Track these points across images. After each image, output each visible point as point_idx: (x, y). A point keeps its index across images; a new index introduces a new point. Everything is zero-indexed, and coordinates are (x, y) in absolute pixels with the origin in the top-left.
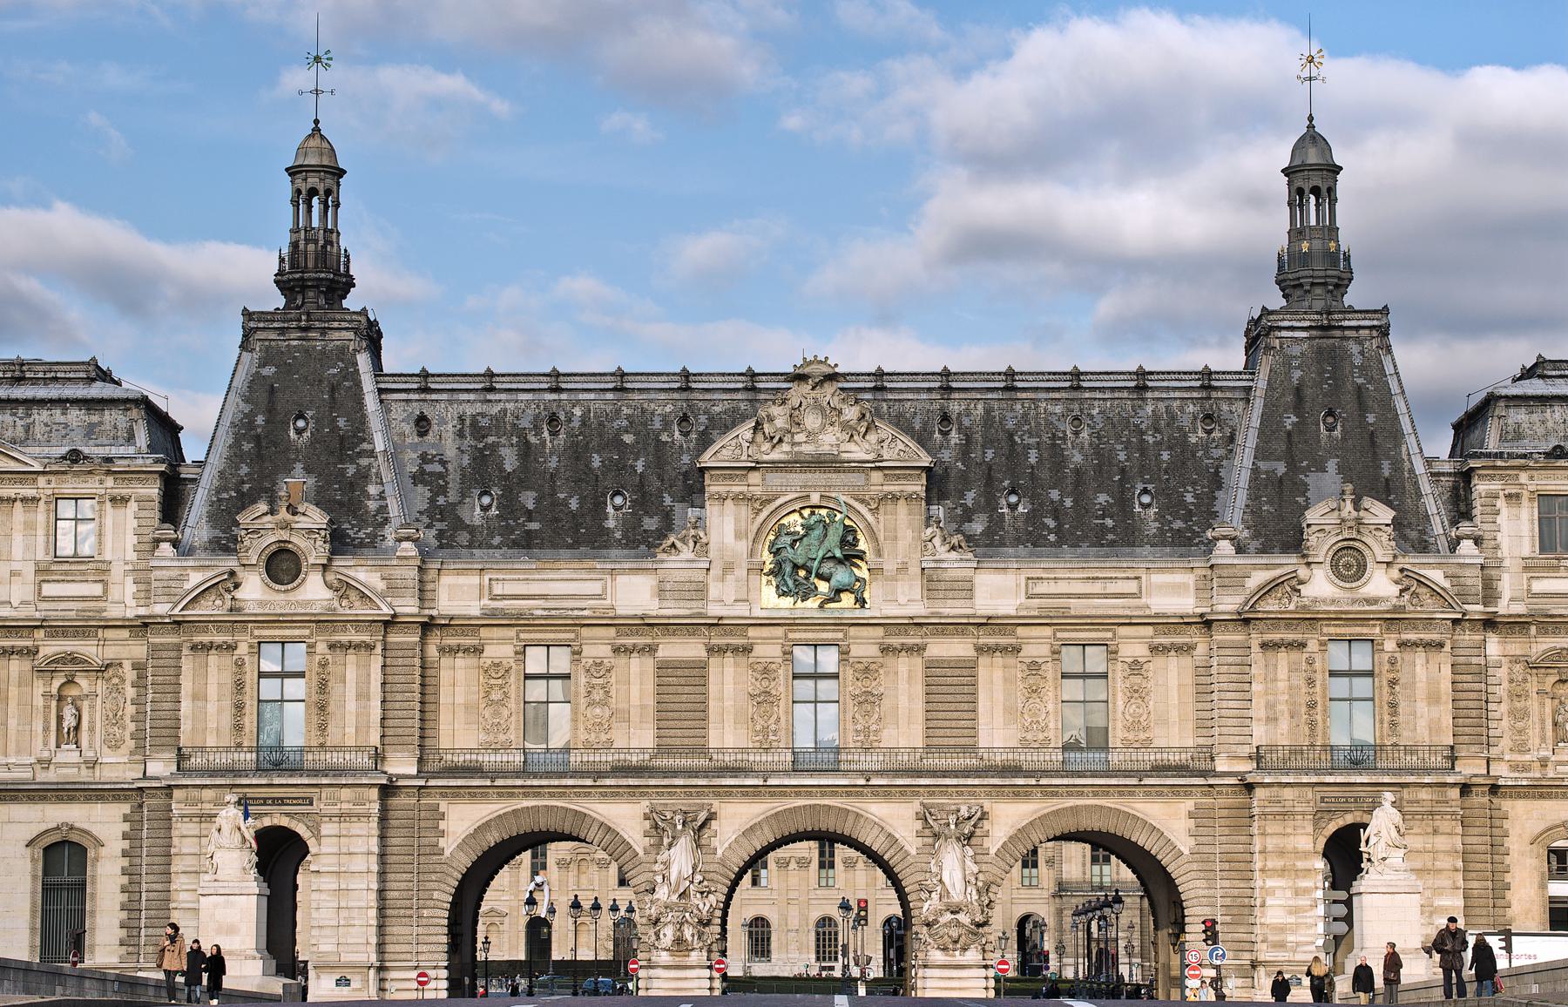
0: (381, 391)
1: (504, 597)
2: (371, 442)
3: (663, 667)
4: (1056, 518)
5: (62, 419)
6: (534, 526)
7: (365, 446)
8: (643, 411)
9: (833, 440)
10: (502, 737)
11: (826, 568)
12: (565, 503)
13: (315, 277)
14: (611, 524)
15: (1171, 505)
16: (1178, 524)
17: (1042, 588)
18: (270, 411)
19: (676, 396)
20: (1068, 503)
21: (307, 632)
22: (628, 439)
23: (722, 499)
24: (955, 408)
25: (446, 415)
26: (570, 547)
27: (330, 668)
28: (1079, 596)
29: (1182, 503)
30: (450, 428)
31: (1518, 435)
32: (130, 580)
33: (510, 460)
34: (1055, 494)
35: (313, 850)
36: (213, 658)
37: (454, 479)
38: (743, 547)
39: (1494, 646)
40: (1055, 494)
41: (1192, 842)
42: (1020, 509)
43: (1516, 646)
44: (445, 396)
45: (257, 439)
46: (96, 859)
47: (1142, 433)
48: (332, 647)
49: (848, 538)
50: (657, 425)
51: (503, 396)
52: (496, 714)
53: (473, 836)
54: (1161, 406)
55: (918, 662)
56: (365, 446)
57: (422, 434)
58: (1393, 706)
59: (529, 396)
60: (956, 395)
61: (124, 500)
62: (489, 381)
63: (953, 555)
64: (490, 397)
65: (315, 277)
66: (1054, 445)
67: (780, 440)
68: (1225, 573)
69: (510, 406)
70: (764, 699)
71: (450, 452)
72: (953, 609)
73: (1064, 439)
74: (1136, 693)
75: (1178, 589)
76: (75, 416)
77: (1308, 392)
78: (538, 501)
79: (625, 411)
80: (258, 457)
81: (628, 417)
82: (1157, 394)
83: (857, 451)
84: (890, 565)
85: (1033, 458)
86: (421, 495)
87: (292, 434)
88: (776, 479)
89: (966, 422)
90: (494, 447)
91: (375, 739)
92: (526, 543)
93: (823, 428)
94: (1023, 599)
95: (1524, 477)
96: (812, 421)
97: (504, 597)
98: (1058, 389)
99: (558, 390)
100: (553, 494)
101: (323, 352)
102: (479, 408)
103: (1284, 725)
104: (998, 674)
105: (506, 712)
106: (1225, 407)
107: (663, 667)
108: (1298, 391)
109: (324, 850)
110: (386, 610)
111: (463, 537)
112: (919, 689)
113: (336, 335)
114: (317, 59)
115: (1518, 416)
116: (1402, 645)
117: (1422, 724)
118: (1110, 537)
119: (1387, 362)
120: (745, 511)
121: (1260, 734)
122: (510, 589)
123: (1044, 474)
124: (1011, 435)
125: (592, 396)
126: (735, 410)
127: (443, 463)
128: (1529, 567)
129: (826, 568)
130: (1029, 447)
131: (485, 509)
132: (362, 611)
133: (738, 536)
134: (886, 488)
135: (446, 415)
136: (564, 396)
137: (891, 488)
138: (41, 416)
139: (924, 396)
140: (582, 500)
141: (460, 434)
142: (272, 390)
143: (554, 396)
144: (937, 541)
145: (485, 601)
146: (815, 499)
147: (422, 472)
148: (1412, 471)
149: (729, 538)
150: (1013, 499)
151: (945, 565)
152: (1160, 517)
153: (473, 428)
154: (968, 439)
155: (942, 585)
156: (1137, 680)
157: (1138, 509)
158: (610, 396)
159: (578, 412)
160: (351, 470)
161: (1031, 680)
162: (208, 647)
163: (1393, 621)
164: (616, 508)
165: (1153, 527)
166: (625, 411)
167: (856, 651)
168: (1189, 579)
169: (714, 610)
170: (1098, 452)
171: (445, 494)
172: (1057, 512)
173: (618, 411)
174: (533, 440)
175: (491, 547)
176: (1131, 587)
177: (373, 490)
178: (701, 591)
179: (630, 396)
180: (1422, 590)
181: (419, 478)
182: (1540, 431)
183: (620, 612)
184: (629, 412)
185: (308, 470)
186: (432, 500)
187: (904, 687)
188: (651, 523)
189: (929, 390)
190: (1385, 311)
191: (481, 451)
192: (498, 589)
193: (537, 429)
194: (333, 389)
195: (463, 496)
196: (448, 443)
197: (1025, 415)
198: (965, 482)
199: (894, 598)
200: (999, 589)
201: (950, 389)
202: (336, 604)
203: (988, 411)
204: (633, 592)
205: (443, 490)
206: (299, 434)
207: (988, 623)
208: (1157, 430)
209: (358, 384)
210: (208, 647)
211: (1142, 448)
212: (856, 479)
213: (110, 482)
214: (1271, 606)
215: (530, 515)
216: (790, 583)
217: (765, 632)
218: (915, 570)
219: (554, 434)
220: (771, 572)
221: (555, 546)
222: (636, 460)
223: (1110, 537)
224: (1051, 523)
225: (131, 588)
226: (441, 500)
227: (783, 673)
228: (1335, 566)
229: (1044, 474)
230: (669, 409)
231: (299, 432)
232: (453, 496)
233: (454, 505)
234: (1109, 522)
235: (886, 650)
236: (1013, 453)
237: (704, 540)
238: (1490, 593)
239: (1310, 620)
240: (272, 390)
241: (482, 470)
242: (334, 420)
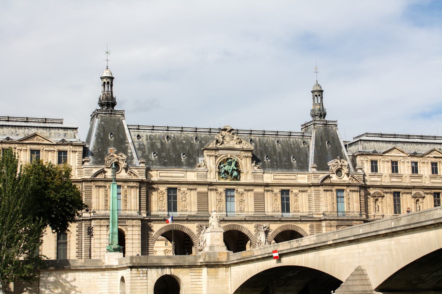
0: (129, 129)
1: (162, 176)
2: (128, 140)
3: (199, 193)
5: (58, 132)
6: (166, 161)
7: (127, 141)
10: (163, 209)
12: (172, 156)
13: (108, 103)
14: (183, 161)
15: (299, 161)
16: (300, 164)
17: (277, 177)
18: (104, 132)
19: (193, 133)
20: (278, 159)
21: (122, 183)
22: (184, 142)
24: (253, 138)
25: (144, 134)
26: (174, 166)
27: (127, 192)
28: (284, 179)
29: (301, 160)
30: (144, 138)
31: (366, 148)
32: (76, 170)
33: (159, 145)
34: (275, 157)
35: (126, 233)
36: (101, 189)
37: (146, 149)
40: (275, 157)
41: (310, 232)
44: (142, 131)
45: (102, 139)
46: (70, 236)
47: (291, 145)
48: (128, 187)
49: (237, 164)
50: (190, 139)
51: (156, 131)
52: (162, 203)
53: (159, 231)
54: (294, 139)
56: (127, 141)
57: (138, 139)
58: (349, 203)
59: (161, 131)
60: (252, 135)
61: (76, 152)
62: (153, 129)
63: (258, 170)
64: (153, 131)
65: (108, 103)
68: (315, 174)
69: (157, 133)
70: (220, 201)
71: (145, 143)
73: (275, 145)
74: (296, 201)
75: (304, 178)
76: (61, 132)
77: (323, 137)
78: (166, 155)
79: (183, 136)
80: (102, 142)
82: (293, 137)
83: (238, 146)
86: (140, 153)
87: (109, 137)
88: (220, 152)
90: (155, 143)
91: (138, 208)
92: (165, 164)
95: (368, 157)
96: (227, 139)
97: (162, 176)
99: (168, 130)
100: (169, 153)
101: (115, 119)
102: (150, 134)
103: (329, 207)
104: (268, 196)
105: (164, 203)
106: (306, 140)
107: (199, 193)
108: (321, 137)
109: (129, 233)
110: (140, 178)
111: (151, 163)
112: (253, 199)
113: (117, 116)
114: (107, 53)
115: (366, 144)
116: (350, 191)
117: (355, 207)
118: (287, 167)
119: (337, 131)
121: (323, 209)
122: (164, 174)
123: (273, 153)
124: (265, 144)
125: (175, 132)
126: (206, 136)
127: (144, 146)
130: (268, 147)
131: (155, 156)
132: (134, 178)
135: (144, 134)
136: (169, 132)
138: (53, 131)
139: (246, 135)
140: (176, 155)
141: (147, 139)
142: (104, 128)
143: (167, 132)
145: (158, 177)
146: (229, 156)
147: (139, 148)
148: (345, 155)
149: (211, 165)
152: (297, 163)
153: (150, 138)
156: (296, 197)
157: (292, 161)
158: (179, 132)
159: (172, 135)
160: (123, 146)
161: (275, 197)
162: (100, 187)
163: (348, 185)
164: (184, 157)
165: (295, 165)
166: (183, 136)
167: (239, 190)
168: (306, 176)
169: (209, 180)
170: (283, 149)
171: (145, 153)
172: (276, 161)
173: (181, 136)
174: (163, 141)
175: (157, 165)
176: (294, 177)
177: (129, 151)
179: (183, 132)
180: (354, 179)
181: (139, 149)
182: (370, 147)
183: (189, 181)
185: (114, 146)
186: (142, 154)
187: (249, 198)
188: (192, 161)
189: (247, 134)
190: (336, 121)
191: (152, 143)
192: (161, 174)
193: (164, 139)
194: (118, 128)
195: (149, 153)
196: (144, 140)
200: (268, 178)
201: (251, 134)
202: (128, 177)
203: (259, 139)
204: (191, 176)
205: (145, 152)
207: (267, 185)
208: (294, 144)
209: (123, 127)
210: (100, 187)
211: (292, 148)
212: (238, 152)
213: (71, 147)
214: (325, 182)
215: (165, 158)
219: (168, 140)
221: (171, 165)
223: (287, 167)
224: (275, 163)
225: (77, 172)
226: (144, 154)
227: (224, 195)
228: (337, 174)
229: (273, 153)
230: (192, 135)
231: (111, 137)
232: (147, 153)
233: (147, 155)
234: (287, 164)
236: (266, 148)
238: (364, 181)
239: (333, 185)
240: (104, 128)
242: (119, 135)
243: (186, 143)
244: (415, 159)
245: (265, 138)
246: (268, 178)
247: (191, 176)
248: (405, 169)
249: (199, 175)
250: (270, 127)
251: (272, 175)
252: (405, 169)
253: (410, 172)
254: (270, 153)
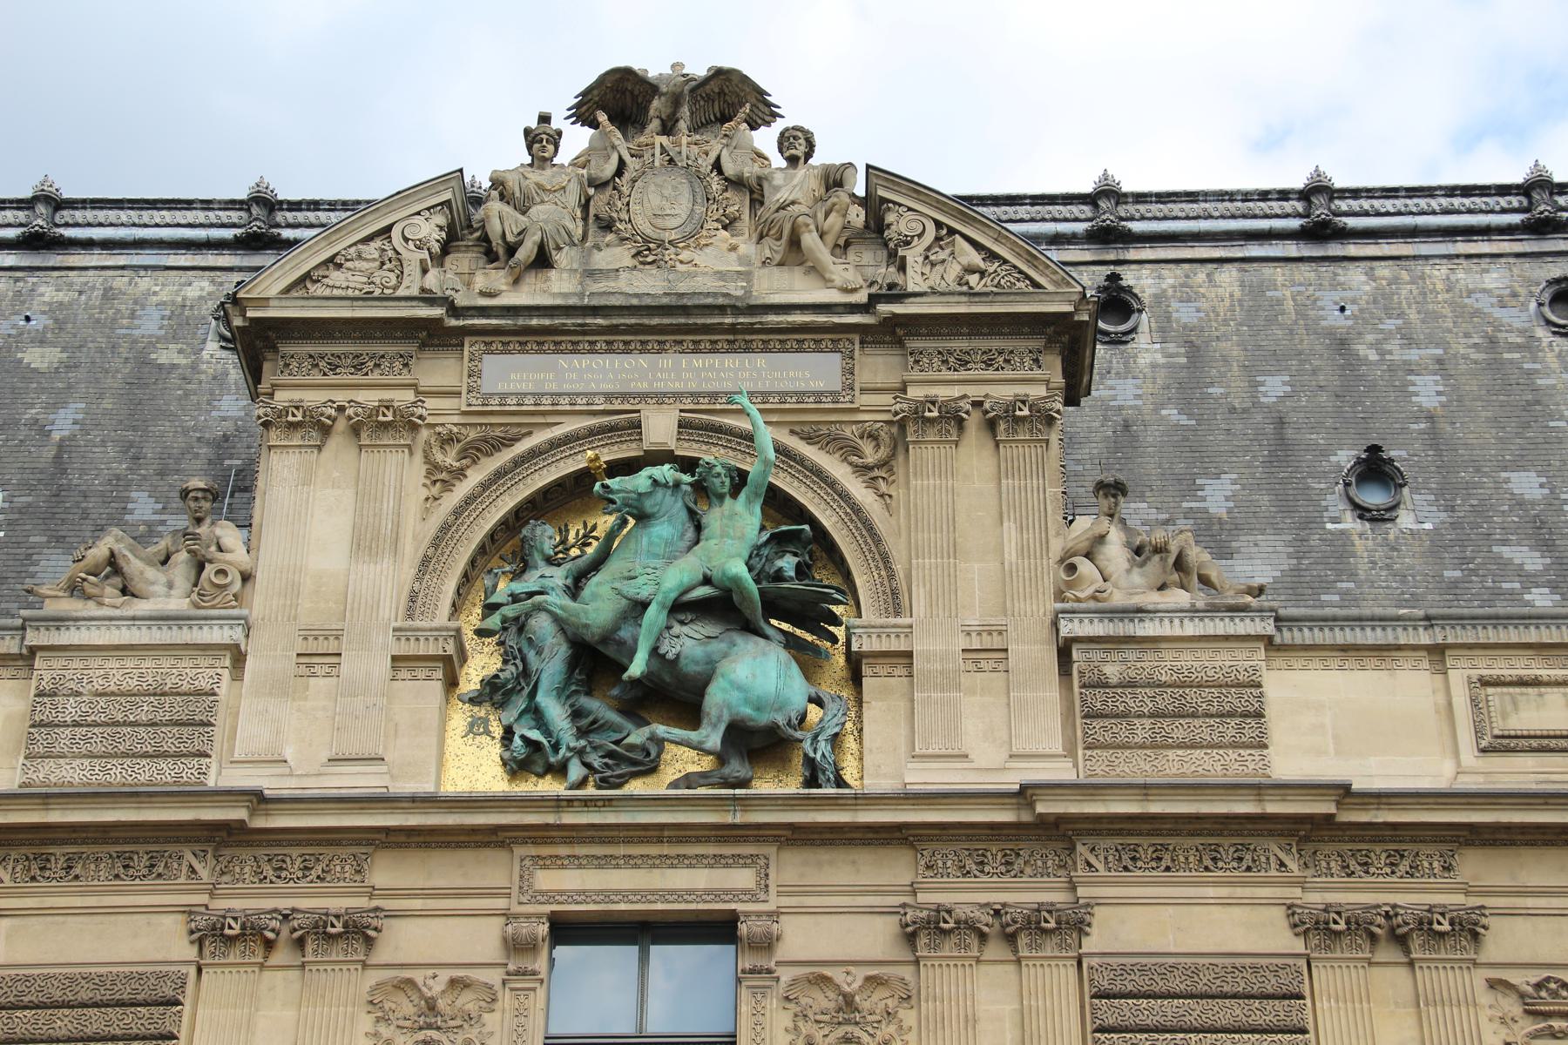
4: (1545, 545)
8: (109, 295)
9: (731, 264)
11: (691, 643)
23: (318, 427)
38: (387, 581)
40: (1527, 484)
42: (1405, 520)
50: (150, 324)
55: (1055, 986)
66: (1495, 365)
67: (542, 260)
81: (53, 309)
84: (934, 642)
85: (1427, 392)
88: (514, 375)
89: (1185, 314)
93: (693, 236)
94: (1469, 756)
96: (660, 202)
98: (1486, 232)
120: (401, 472)
124: (1341, 344)
129: (691, 643)
133: (365, 543)
134: (914, 392)
137: (943, 392)
144: (1115, 552)
146: (660, 428)
150: (1374, 497)
151: (1149, 628)
154: (1196, 351)
155: (1143, 700)
178: (195, 721)
184: (61, 296)
197: (1384, 302)
198: (1195, 457)
203: (1256, 291)
212: (813, 372)
216: (556, 713)
217: (446, 870)
218: (1032, 652)
220: (494, 692)
222: (55, 406)
235: (924, 931)
237: (237, 554)
243: (71, 366)
245: (1355, 276)
249: (71, 709)
251: (1460, 674)
254: (1434, 438)
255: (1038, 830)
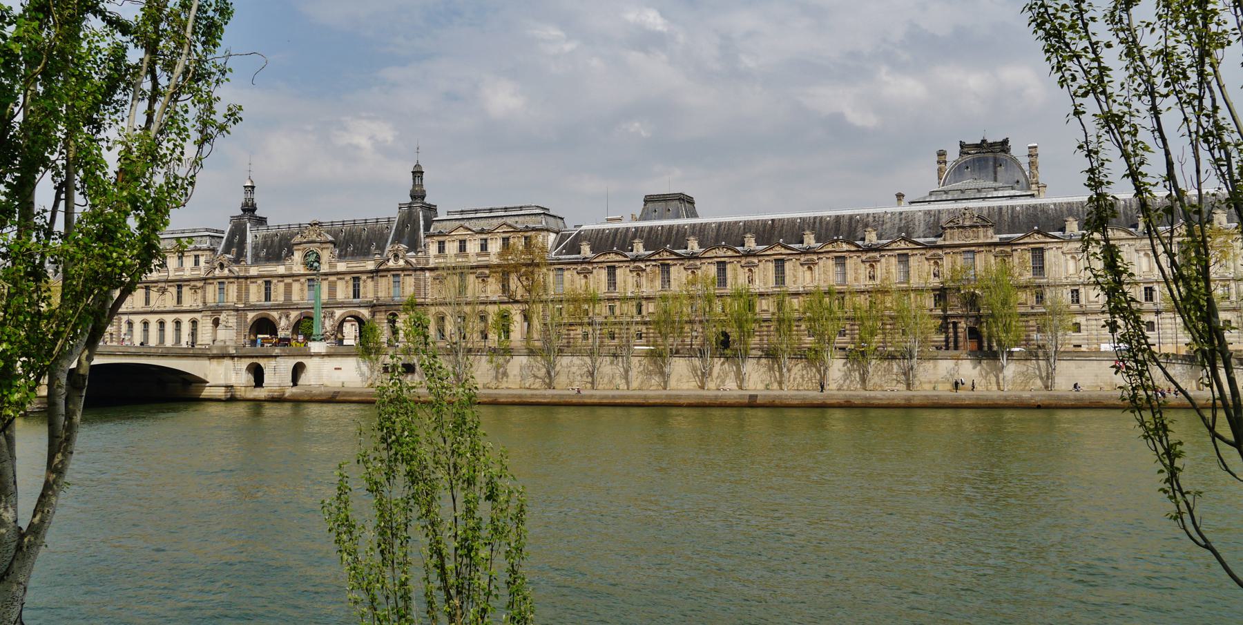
39: (428, 274)
43: (433, 274)
70: (302, 290)
72: (333, 270)
128: (436, 257)
187: (325, 286)
196: (260, 239)
199: (325, 268)
206: (236, 241)
238: (428, 263)
239: (388, 270)
241: (265, 245)
244: (484, 236)
246: (341, 267)
247: (281, 270)
248: (473, 247)
250: (360, 217)
252: (473, 247)
253: (478, 250)
255: (326, 274)
